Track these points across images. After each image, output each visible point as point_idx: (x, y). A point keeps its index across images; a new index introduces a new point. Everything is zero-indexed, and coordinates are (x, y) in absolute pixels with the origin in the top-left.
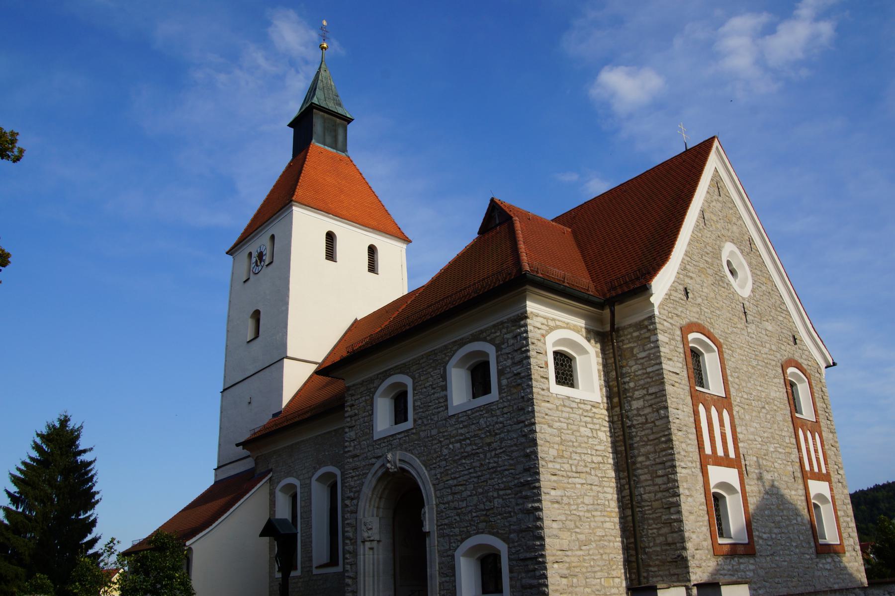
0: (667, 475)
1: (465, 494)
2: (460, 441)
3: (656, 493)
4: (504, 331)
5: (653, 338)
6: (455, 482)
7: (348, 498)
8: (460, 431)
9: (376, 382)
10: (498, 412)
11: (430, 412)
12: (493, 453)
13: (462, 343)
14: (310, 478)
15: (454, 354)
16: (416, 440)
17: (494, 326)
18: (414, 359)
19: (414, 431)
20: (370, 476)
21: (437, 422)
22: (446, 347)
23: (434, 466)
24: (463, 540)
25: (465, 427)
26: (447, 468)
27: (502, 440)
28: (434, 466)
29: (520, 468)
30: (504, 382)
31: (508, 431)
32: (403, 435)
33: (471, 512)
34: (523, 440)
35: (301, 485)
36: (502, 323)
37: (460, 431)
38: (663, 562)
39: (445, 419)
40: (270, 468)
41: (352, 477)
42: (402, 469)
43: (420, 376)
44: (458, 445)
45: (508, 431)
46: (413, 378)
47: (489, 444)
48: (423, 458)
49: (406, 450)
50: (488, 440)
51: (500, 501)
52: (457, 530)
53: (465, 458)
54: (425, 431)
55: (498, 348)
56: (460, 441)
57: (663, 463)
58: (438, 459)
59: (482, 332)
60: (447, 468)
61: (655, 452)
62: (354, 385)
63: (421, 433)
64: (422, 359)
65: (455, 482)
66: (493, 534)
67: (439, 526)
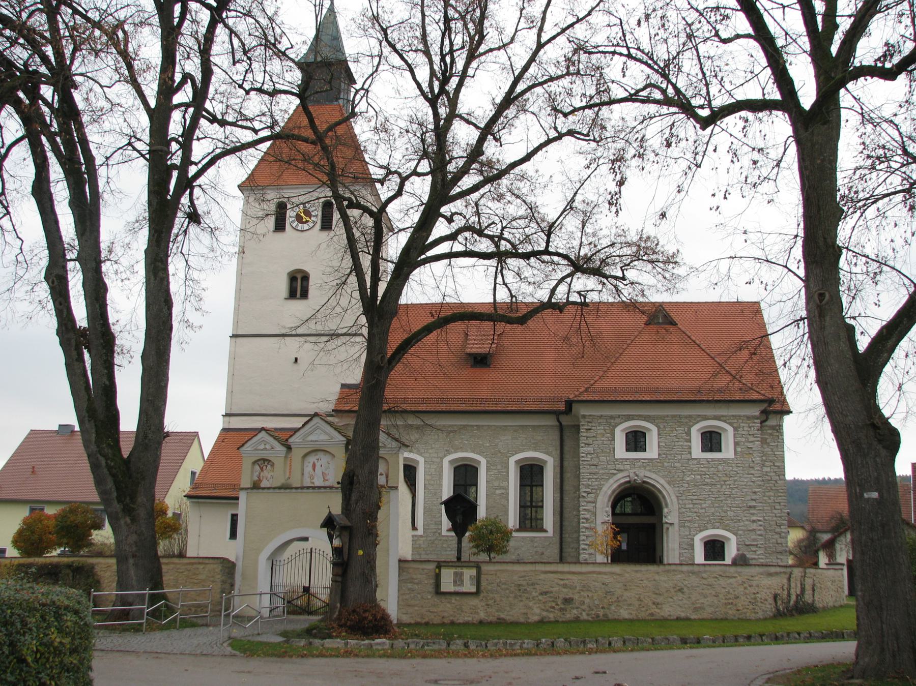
0: (781, 509)
1: (704, 506)
2: (701, 475)
3: (772, 517)
4: (741, 421)
5: (780, 437)
6: (696, 497)
7: (585, 492)
8: (700, 469)
9: (617, 420)
10: (734, 465)
12: (728, 487)
13: (706, 418)
14: (442, 459)
15: (697, 423)
17: (733, 416)
20: (611, 481)
22: (690, 416)
24: (701, 531)
25: (704, 467)
27: (735, 481)
29: (748, 498)
30: (739, 449)
31: (740, 477)
33: (708, 516)
34: (752, 484)
36: (740, 416)
37: (700, 469)
38: (773, 552)
39: (688, 460)
41: (589, 479)
42: (644, 482)
43: (665, 427)
44: (699, 477)
45: (740, 477)
46: (659, 428)
47: (725, 481)
49: (650, 471)
50: (724, 479)
51: (732, 513)
52: (696, 525)
53: (704, 485)
55: (735, 429)
56: (701, 475)
57: (779, 503)
59: (723, 416)
61: (775, 496)
62: (590, 416)
65: (696, 497)
66: (726, 530)
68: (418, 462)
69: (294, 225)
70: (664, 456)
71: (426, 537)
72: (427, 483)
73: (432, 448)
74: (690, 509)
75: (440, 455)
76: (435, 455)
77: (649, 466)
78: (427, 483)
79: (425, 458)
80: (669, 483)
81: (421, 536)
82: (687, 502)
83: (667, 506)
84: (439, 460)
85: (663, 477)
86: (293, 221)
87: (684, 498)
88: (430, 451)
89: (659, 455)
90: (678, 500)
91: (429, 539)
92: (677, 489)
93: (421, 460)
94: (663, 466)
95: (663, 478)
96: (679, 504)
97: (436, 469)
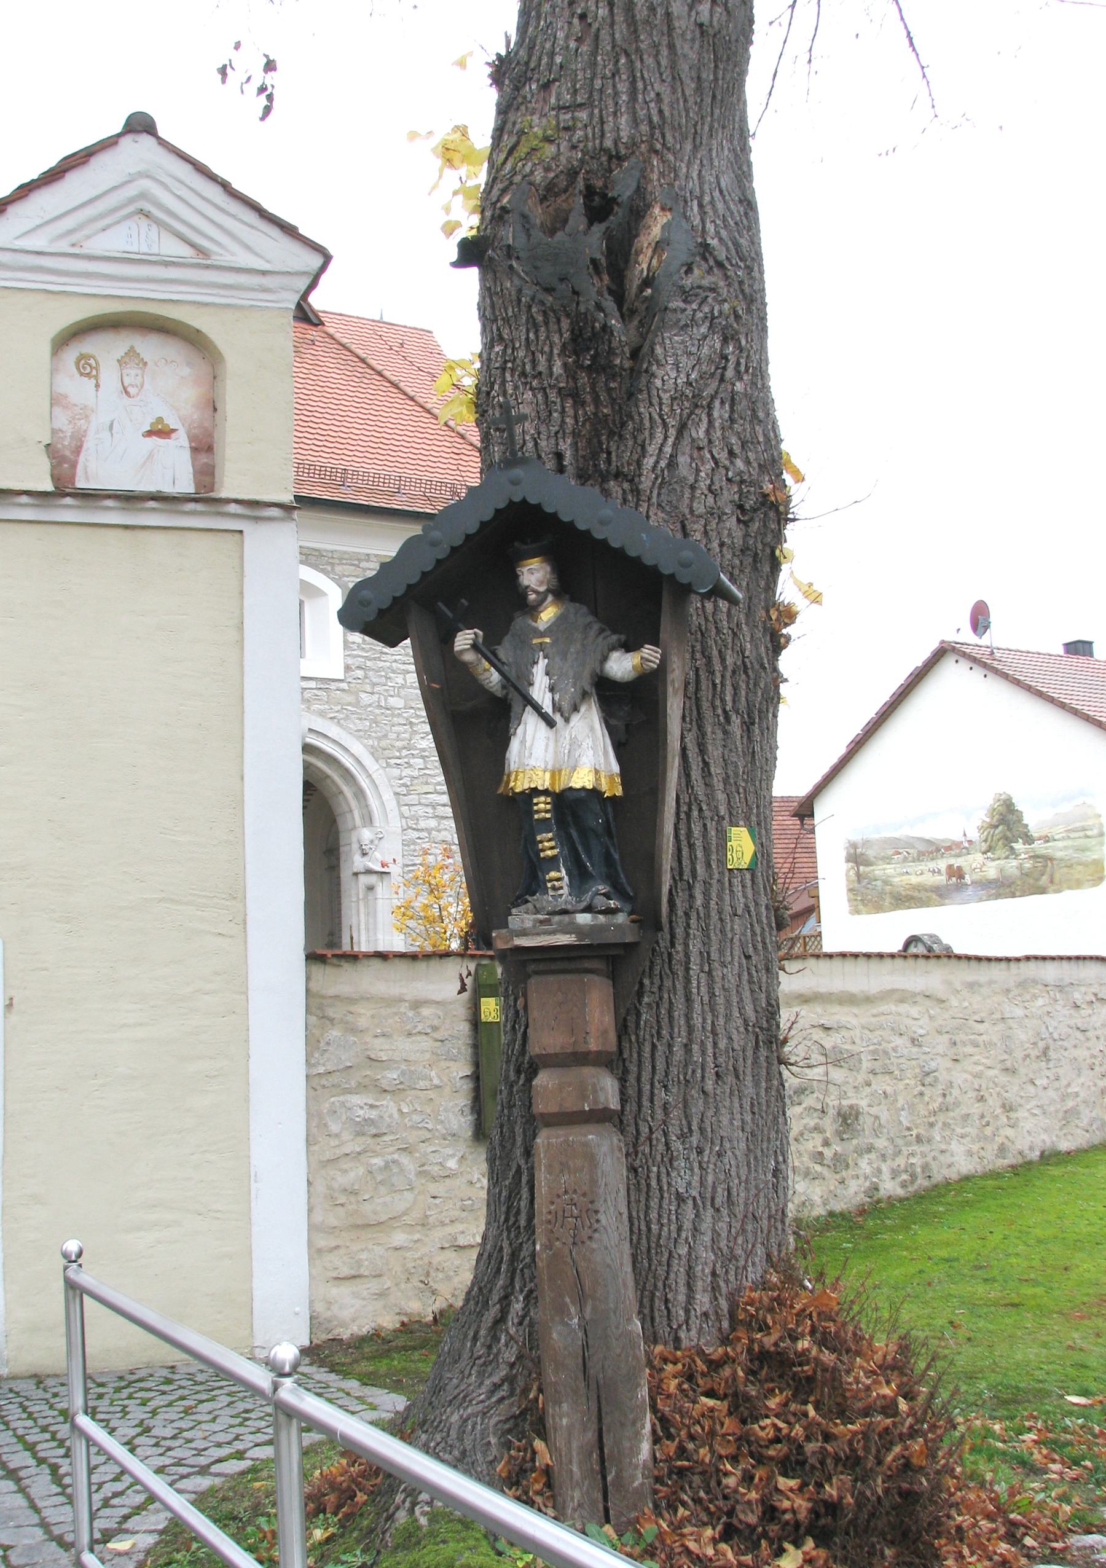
11: (388, 664)
16: (349, 704)
18: (345, 552)
19: (344, 686)
21: (403, 686)
23: (398, 761)
26: (427, 772)
28: (398, 761)
32: (313, 684)
48: (371, 742)
49: (322, 714)
54: (372, 693)
58: (405, 752)
60: (427, 772)
63: (363, 695)
64: (368, 561)
67: (408, 866)
70: (360, 673)
74: (429, 831)
77: (318, 698)
80: (374, 753)
82: (420, 810)
83: (368, 820)
85: (360, 735)
87: (413, 798)
89: (347, 668)
90: (399, 805)
92: (396, 772)
94: (357, 704)
95: (359, 738)
96: (402, 816)
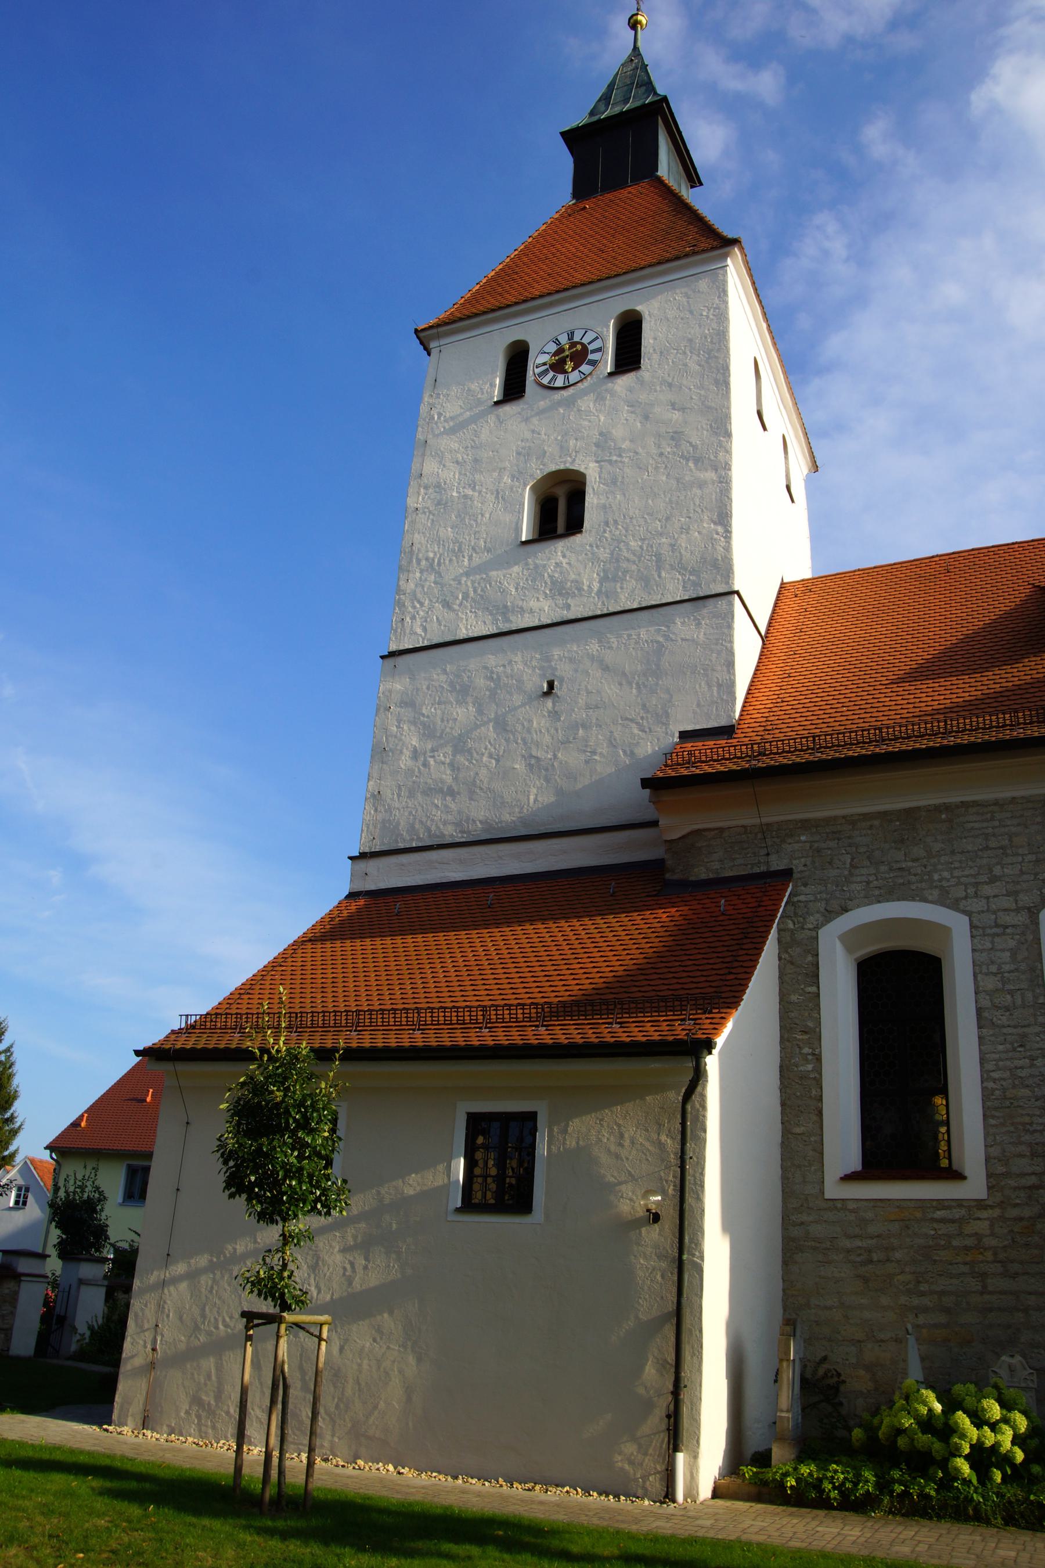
35: (972, 926)
40: (777, 864)
68: (944, 932)
69: (545, 381)
71: (1001, 1205)
72: (986, 1003)
73: (993, 880)
75: (1025, 900)
76: (1007, 902)
78: (986, 1003)
79: (968, 913)
81: (980, 1204)
84: (1022, 918)
86: (544, 373)
88: (987, 890)
91: (1013, 1213)
93: (958, 924)
97: (1014, 952)
